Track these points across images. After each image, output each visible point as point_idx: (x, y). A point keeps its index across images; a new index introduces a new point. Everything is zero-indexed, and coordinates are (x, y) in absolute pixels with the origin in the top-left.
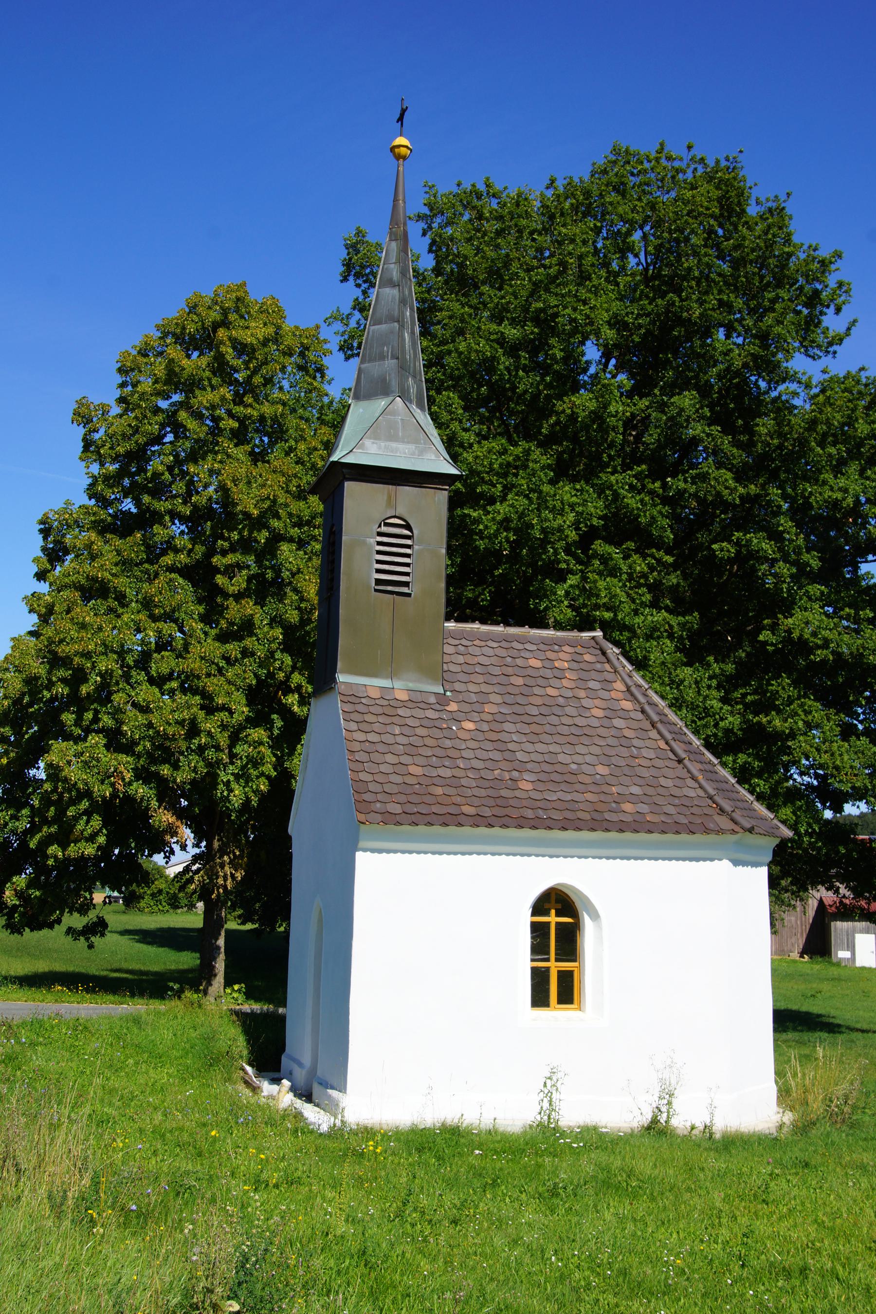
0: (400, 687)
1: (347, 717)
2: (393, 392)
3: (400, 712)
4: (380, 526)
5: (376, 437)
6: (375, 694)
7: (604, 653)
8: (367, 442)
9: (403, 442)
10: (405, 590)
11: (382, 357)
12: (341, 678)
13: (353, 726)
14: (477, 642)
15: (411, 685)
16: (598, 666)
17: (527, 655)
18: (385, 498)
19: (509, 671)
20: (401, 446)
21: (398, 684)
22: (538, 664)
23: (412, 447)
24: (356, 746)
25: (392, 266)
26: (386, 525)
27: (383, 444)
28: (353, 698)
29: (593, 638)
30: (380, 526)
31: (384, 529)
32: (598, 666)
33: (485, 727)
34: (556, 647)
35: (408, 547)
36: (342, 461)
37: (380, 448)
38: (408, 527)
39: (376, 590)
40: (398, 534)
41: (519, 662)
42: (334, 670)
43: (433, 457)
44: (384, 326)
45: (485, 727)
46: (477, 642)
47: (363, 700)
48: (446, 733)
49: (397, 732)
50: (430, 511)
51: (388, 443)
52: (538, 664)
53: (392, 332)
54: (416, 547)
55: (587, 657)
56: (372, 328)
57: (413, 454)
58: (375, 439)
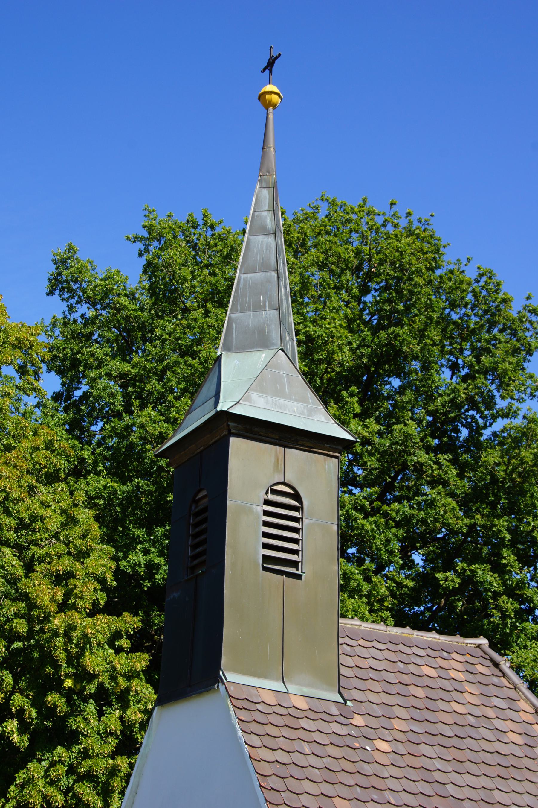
0: (299, 692)
1: (246, 727)
2: (273, 344)
3: (304, 723)
4: (267, 493)
5: (263, 391)
6: (271, 699)
7: (496, 665)
8: (254, 396)
9: (291, 399)
10: (293, 570)
11: (258, 307)
12: (231, 677)
13: (256, 741)
14: (361, 642)
15: (307, 691)
16: (495, 680)
17: (418, 661)
18: (273, 459)
19: (406, 679)
20: (290, 404)
21: (292, 688)
22: (433, 673)
23: (301, 405)
24: (266, 769)
25: (265, 214)
26: (274, 492)
27: (270, 399)
28: (246, 703)
29: (479, 646)
30: (267, 493)
31: (271, 497)
32: (495, 680)
33: (401, 749)
34: (445, 654)
35: (296, 519)
36: (232, 411)
37: (267, 403)
38: (296, 496)
39: (264, 569)
40: (285, 505)
41: (412, 668)
42: (218, 665)
43: (323, 419)
44: (259, 274)
45: (401, 749)
46: (361, 642)
47: (259, 707)
48: (361, 754)
49: (307, 751)
50: (317, 479)
51: (275, 399)
52: (433, 673)
53: (269, 281)
54: (306, 521)
55: (480, 668)
56: (243, 276)
57: (302, 413)
58: (262, 392)
